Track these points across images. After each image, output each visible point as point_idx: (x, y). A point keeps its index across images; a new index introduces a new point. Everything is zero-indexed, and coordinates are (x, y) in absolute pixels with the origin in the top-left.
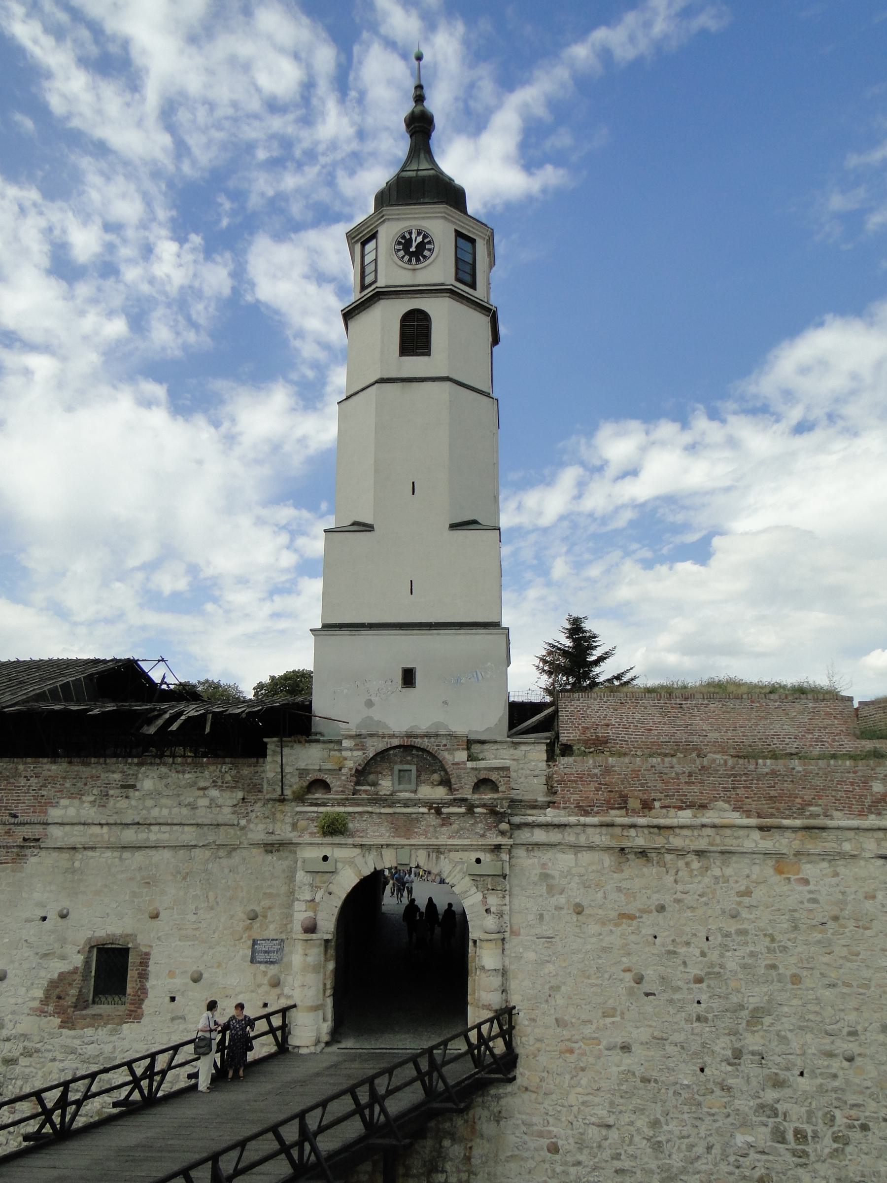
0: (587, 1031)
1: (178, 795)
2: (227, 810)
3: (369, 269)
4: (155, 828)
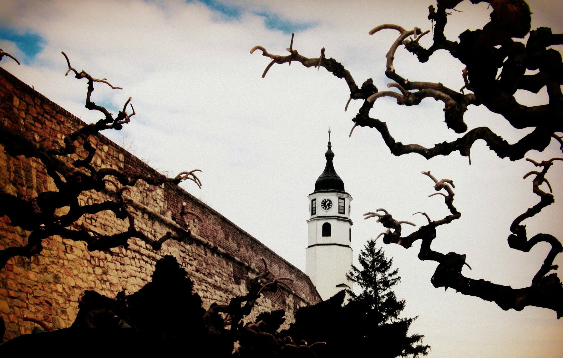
3: (314, 209)
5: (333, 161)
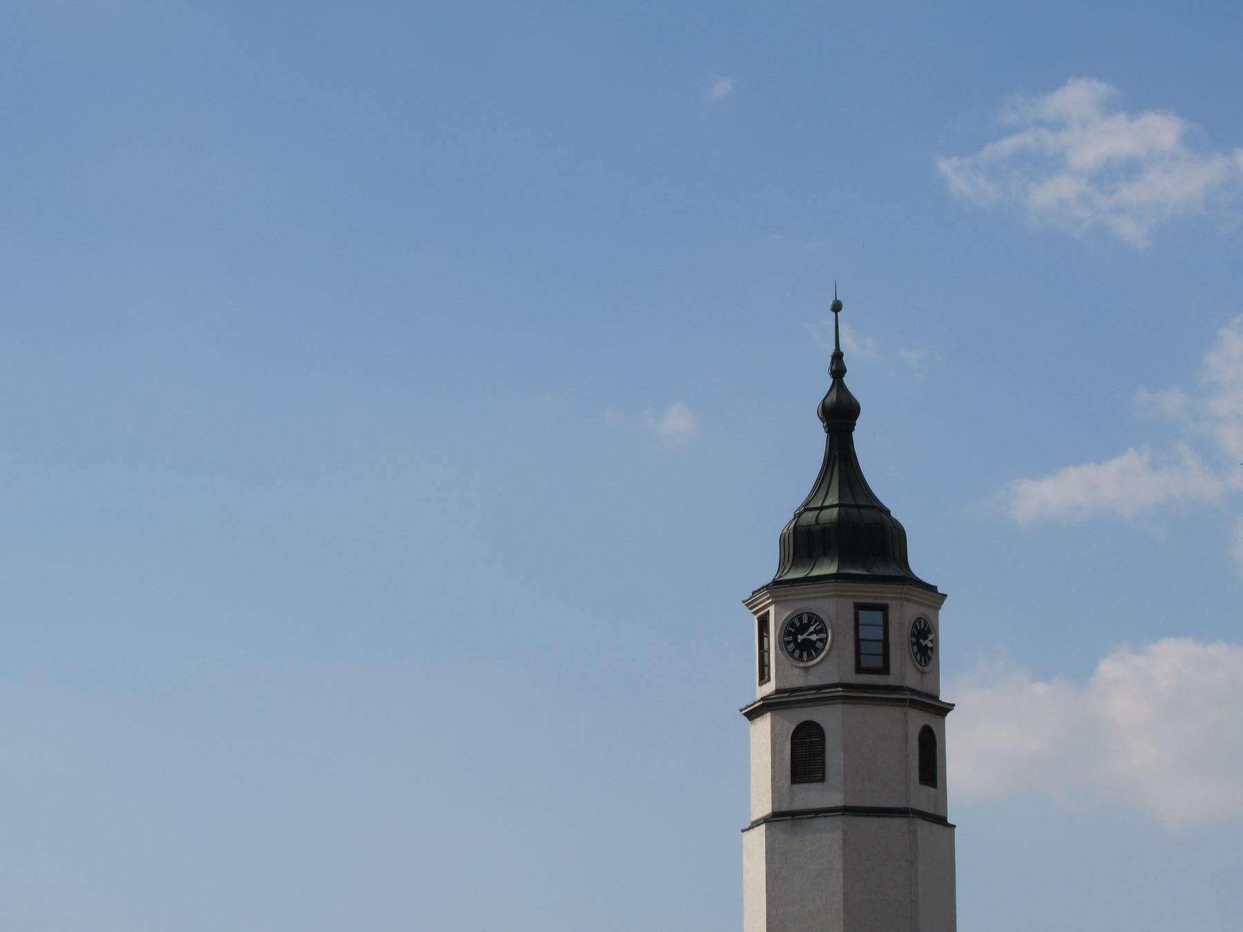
5: (856, 435)
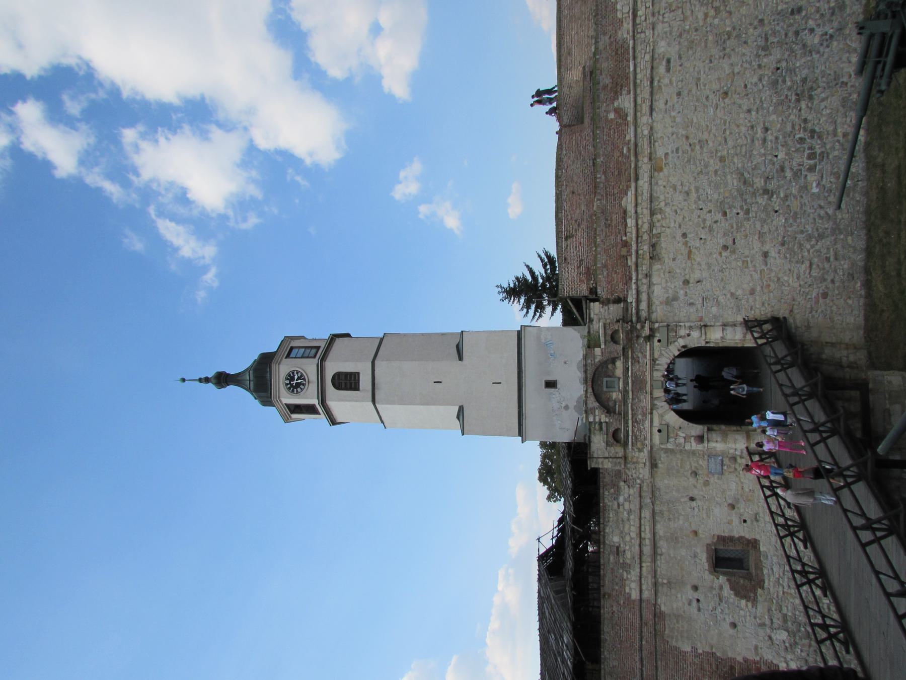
0: (756, 276)
1: (623, 521)
2: (632, 491)
4: (643, 535)
